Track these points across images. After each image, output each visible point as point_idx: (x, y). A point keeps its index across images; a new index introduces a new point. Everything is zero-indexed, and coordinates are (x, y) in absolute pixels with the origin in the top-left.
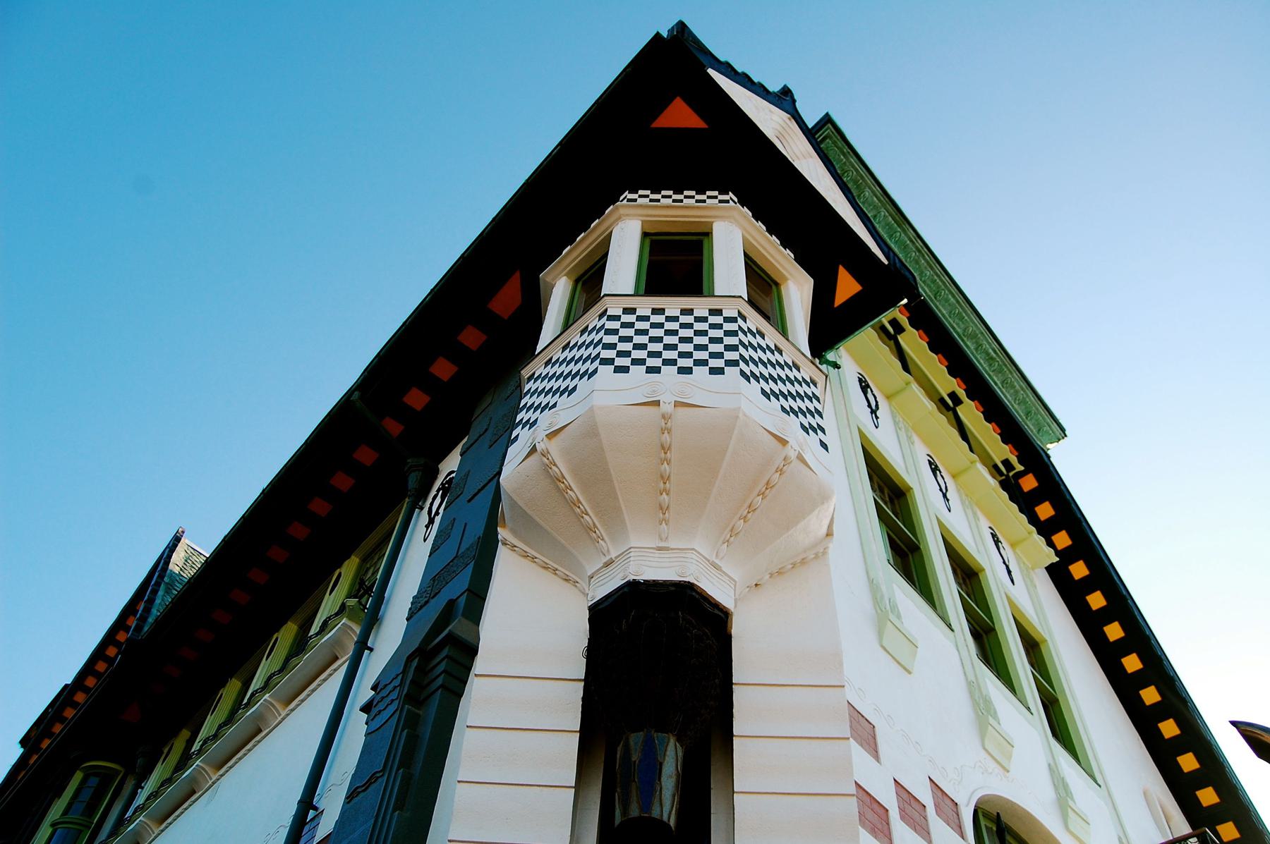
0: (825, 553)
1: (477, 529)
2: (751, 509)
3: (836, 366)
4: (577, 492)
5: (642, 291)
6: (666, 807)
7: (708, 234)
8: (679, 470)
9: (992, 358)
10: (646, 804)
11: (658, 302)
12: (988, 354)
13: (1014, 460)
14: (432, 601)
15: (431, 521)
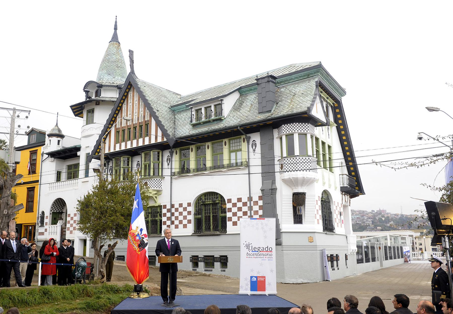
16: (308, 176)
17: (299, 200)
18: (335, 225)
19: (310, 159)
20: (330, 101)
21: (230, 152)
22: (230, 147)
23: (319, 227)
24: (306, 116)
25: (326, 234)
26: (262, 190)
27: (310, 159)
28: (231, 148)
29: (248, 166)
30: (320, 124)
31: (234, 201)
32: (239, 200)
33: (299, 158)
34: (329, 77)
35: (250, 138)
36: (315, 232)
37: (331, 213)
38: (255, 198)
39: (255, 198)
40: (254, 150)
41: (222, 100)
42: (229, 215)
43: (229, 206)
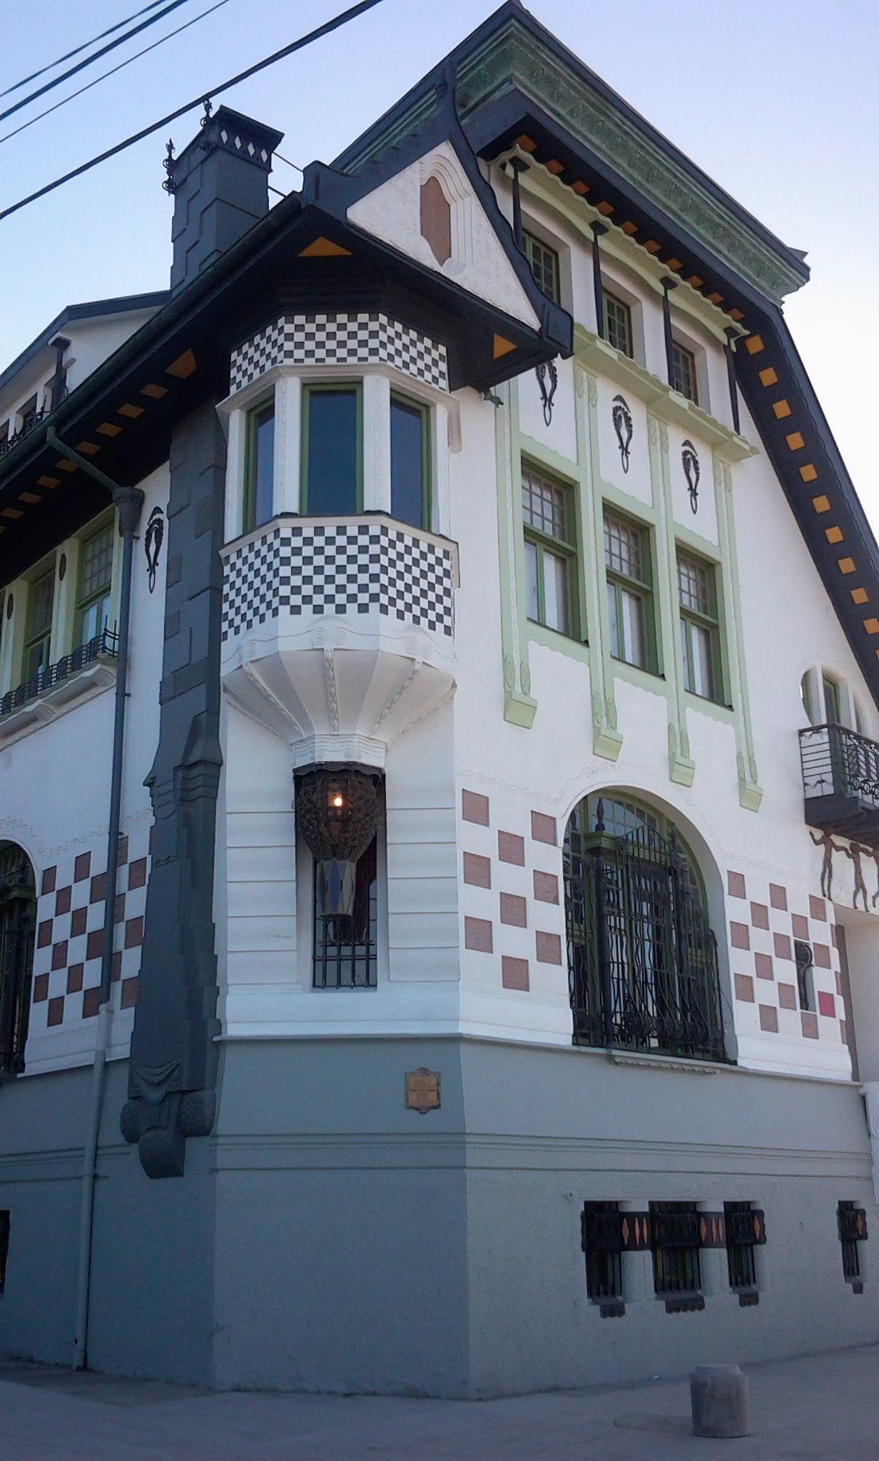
0: (452, 698)
1: (201, 651)
2: (393, 702)
3: (498, 402)
4: (275, 698)
5: (305, 512)
6: (346, 905)
7: (360, 382)
8: (345, 683)
9: (718, 225)
10: (335, 908)
11: (319, 522)
12: (711, 221)
13: (738, 326)
14: (179, 699)
15: (152, 569)
16: (351, 643)
17: (342, 822)
18: (743, 1019)
19: (375, 530)
20: (716, 321)
21: (82, 605)
22: (81, 580)
23: (546, 1012)
24: (322, 247)
25: (611, 1059)
26: (150, 783)
27: (375, 530)
28: (88, 585)
29: (122, 660)
30: (502, 346)
31: (64, 878)
32: (82, 863)
33: (297, 531)
34: (617, 117)
35: (140, 499)
36: (457, 1039)
37: (708, 942)
38: (138, 847)
39: (138, 847)
40: (152, 569)
41: (63, 345)
42: (42, 960)
43: (45, 907)
